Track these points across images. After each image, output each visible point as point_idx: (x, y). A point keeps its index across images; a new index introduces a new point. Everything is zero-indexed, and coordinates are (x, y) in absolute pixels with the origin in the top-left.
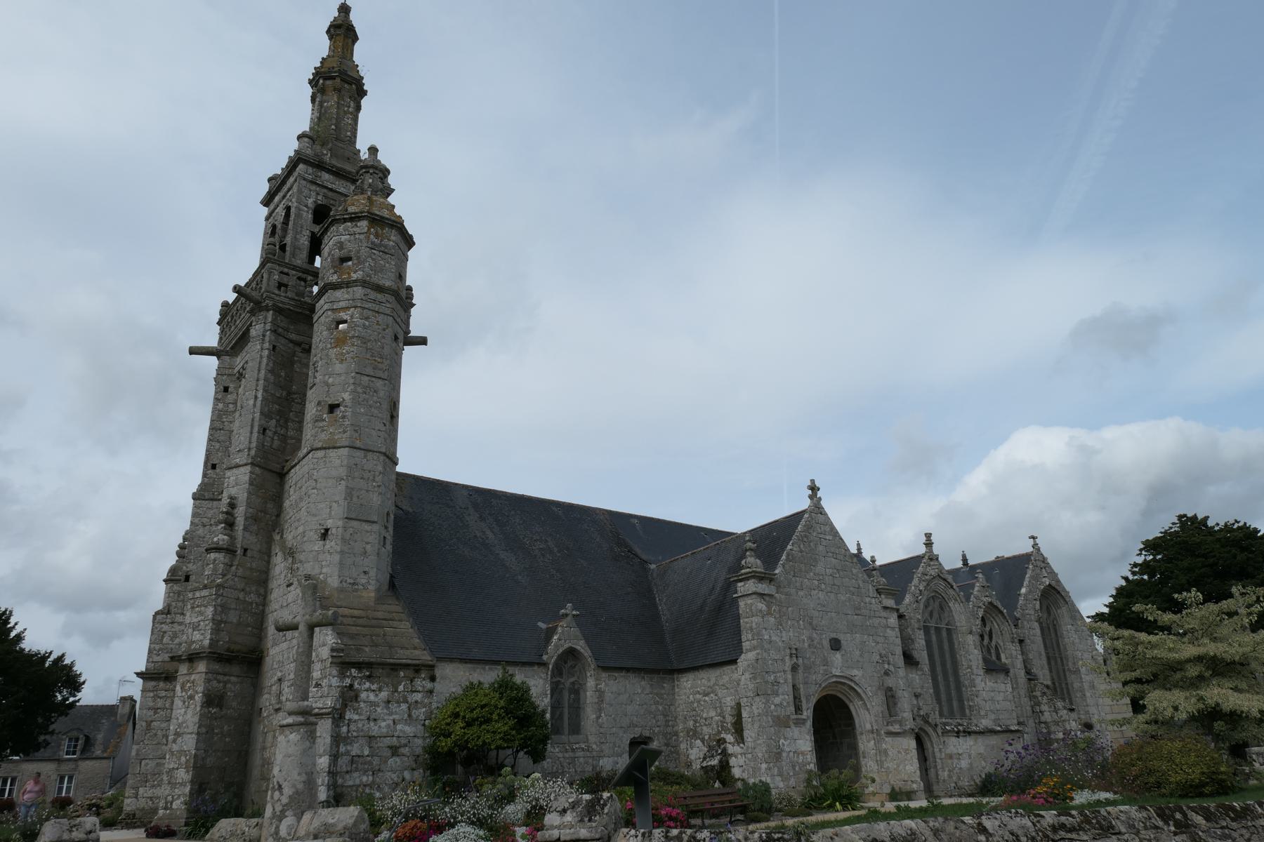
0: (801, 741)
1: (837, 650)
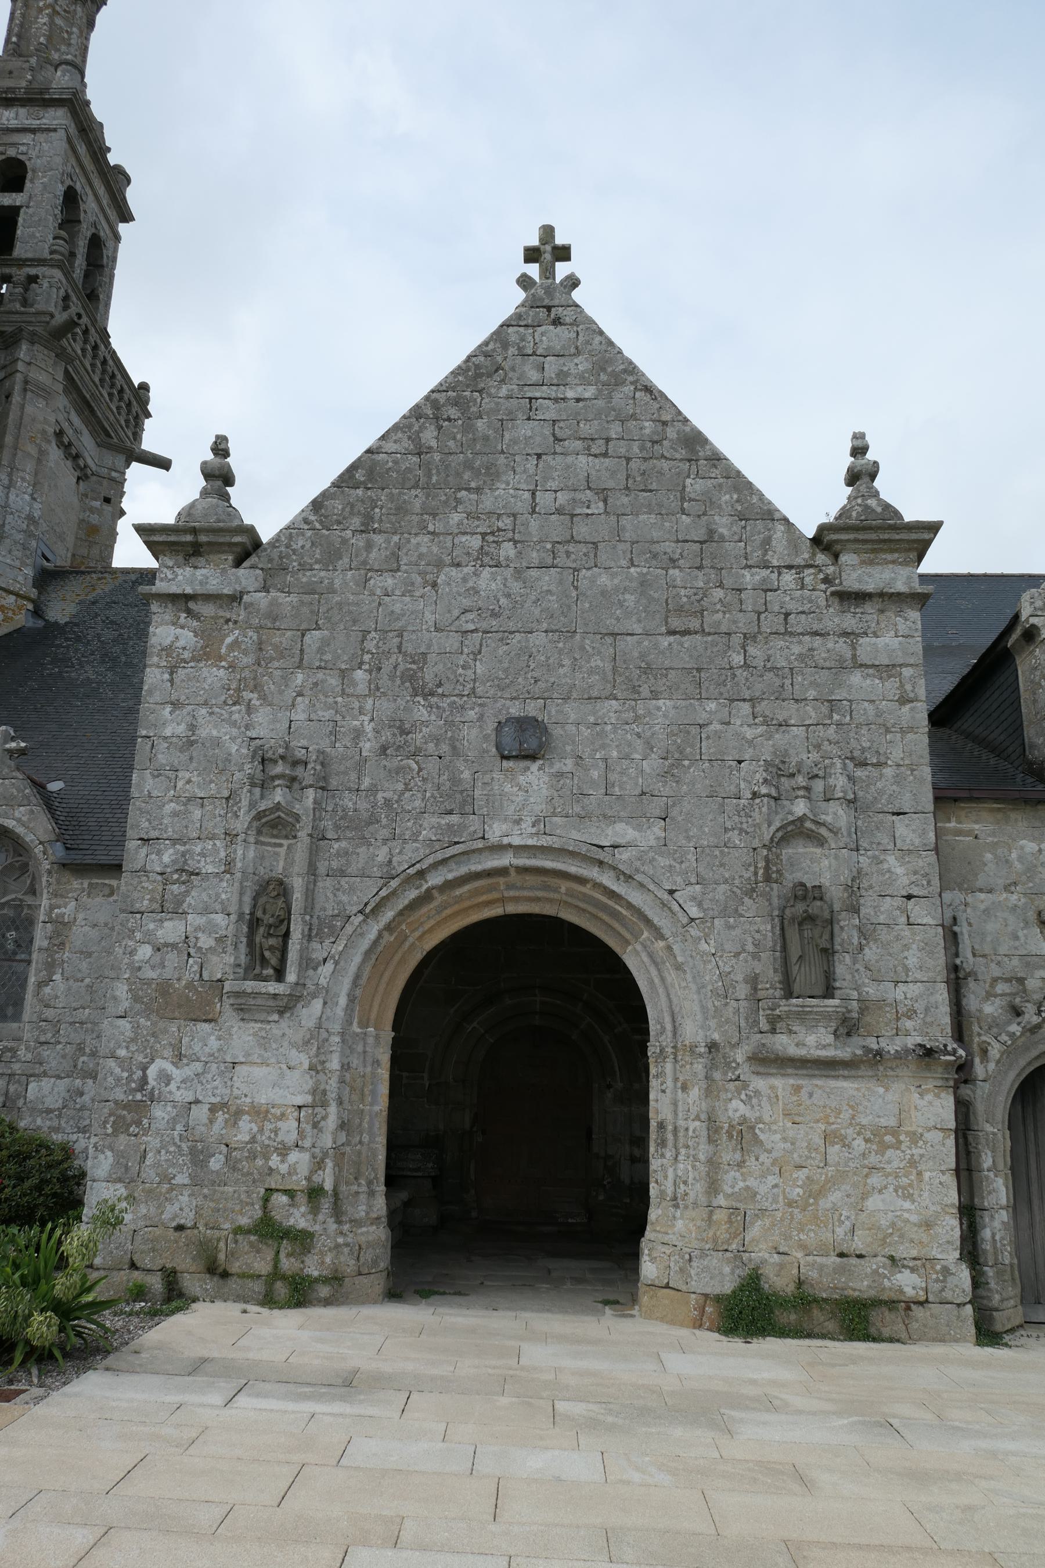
0: (258, 1072)
1: (533, 757)
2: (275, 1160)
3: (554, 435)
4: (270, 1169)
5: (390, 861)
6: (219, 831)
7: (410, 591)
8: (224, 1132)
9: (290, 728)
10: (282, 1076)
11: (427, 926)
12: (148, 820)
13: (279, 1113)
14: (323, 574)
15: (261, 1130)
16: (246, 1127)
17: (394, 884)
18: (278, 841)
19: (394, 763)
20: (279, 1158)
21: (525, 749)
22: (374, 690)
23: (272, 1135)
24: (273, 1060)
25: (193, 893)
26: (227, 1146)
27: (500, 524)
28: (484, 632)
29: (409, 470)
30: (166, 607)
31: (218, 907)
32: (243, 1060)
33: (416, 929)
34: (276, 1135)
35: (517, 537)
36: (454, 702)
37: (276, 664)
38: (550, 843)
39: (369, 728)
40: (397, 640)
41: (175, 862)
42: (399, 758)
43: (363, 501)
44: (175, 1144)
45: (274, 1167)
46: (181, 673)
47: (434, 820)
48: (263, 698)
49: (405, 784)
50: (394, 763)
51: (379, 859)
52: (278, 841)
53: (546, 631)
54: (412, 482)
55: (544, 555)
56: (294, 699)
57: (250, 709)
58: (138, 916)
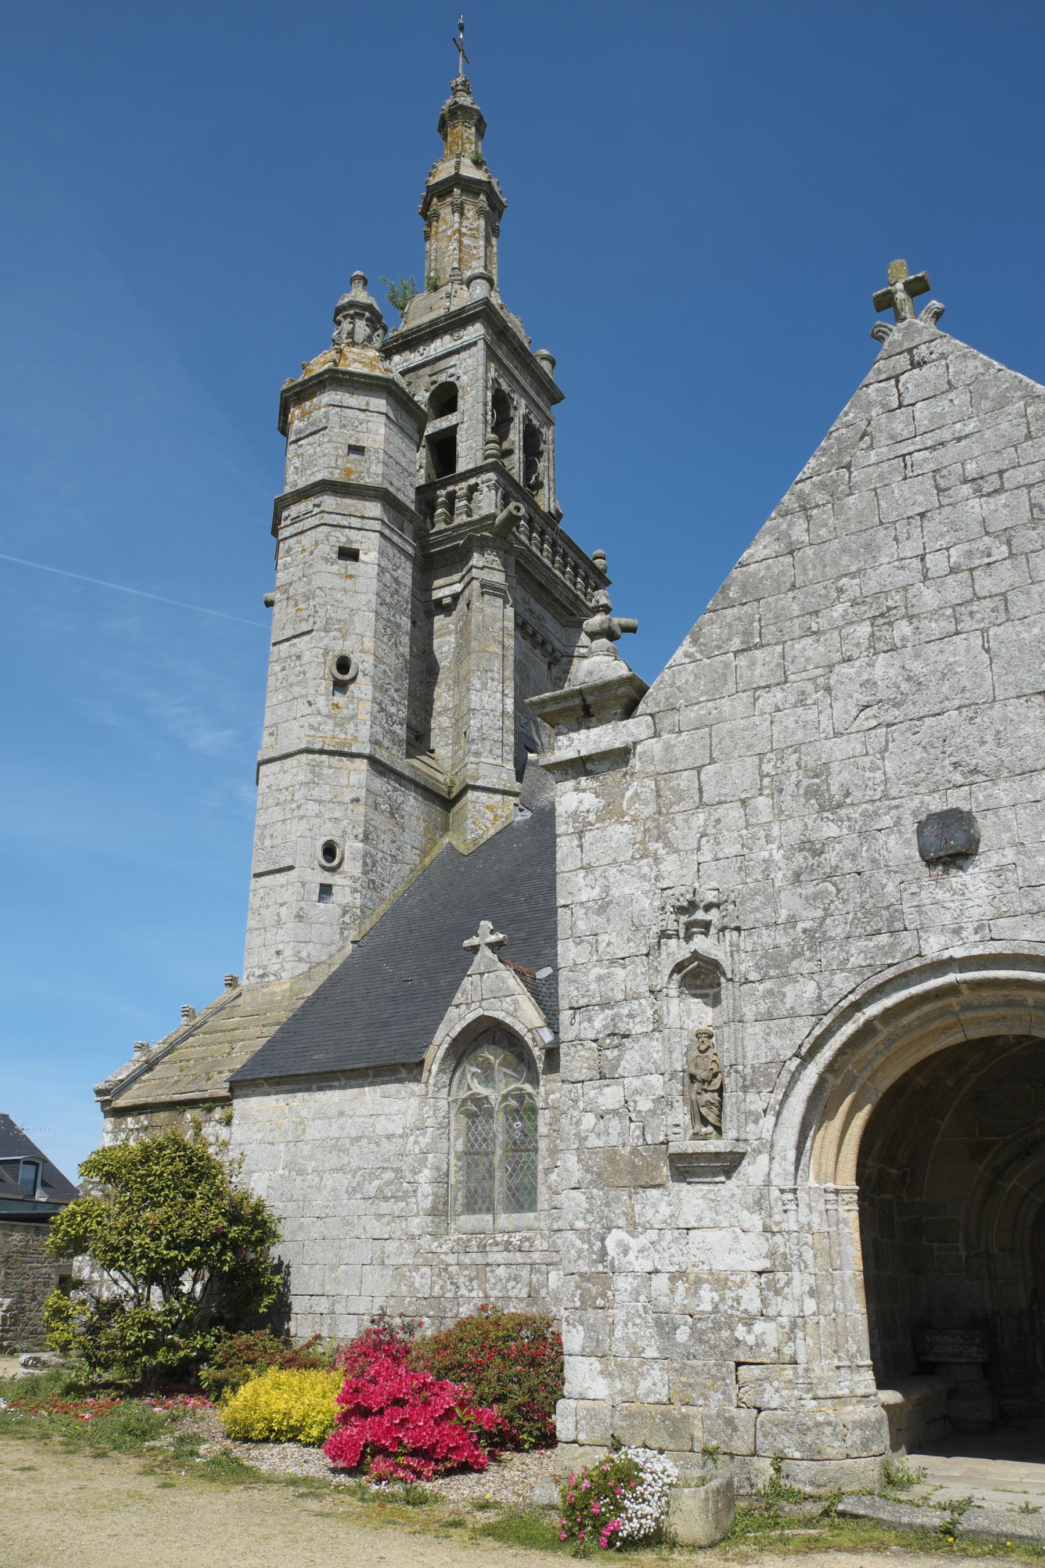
0: (712, 1237)
2: (740, 1331)
3: (937, 487)
4: (737, 1340)
5: (819, 997)
6: (644, 989)
7: (802, 701)
8: (686, 1302)
9: (698, 871)
10: (736, 1239)
11: (876, 1064)
12: (577, 989)
13: (738, 1281)
14: (710, 704)
15: (723, 1299)
16: (707, 1297)
17: (827, 1020)
18: (703, 991)
19: (810, 889)
20: (745, 1329)
21: (953, 846)
22: (779, 812)
23: (735, 1304)
24: (725, 1224)
25: (627, 1057)
26: (691, 1316)
27: (890, 603)
28: (889, 725)
29: (782, 573)
30: (567, 774)
31: (653, 1068)
32: (695, 1225)
33: (865, 1069)
34: (739, 1303)
35: (911, 611)
36: (866, 810)
37: (676, 808)
38: (1000, 950)
39: (778, 856)
40: (795, 757)
41: (605, 1027)
42: (814, 883)
43: (740, 619)
44: (640, 1316)
45: (741, 1338)
46: (588, 836)
47: (862, 943)
48: (668, 844)
49: (825, 909)
50: (810, 889)
51: (806, 995)
52: (703, 991)
53: (959, 708)
54: (788, 586)
55: (943, 624)
56: (699, 842)
57: (657, 860)
58: (579, 1085)
